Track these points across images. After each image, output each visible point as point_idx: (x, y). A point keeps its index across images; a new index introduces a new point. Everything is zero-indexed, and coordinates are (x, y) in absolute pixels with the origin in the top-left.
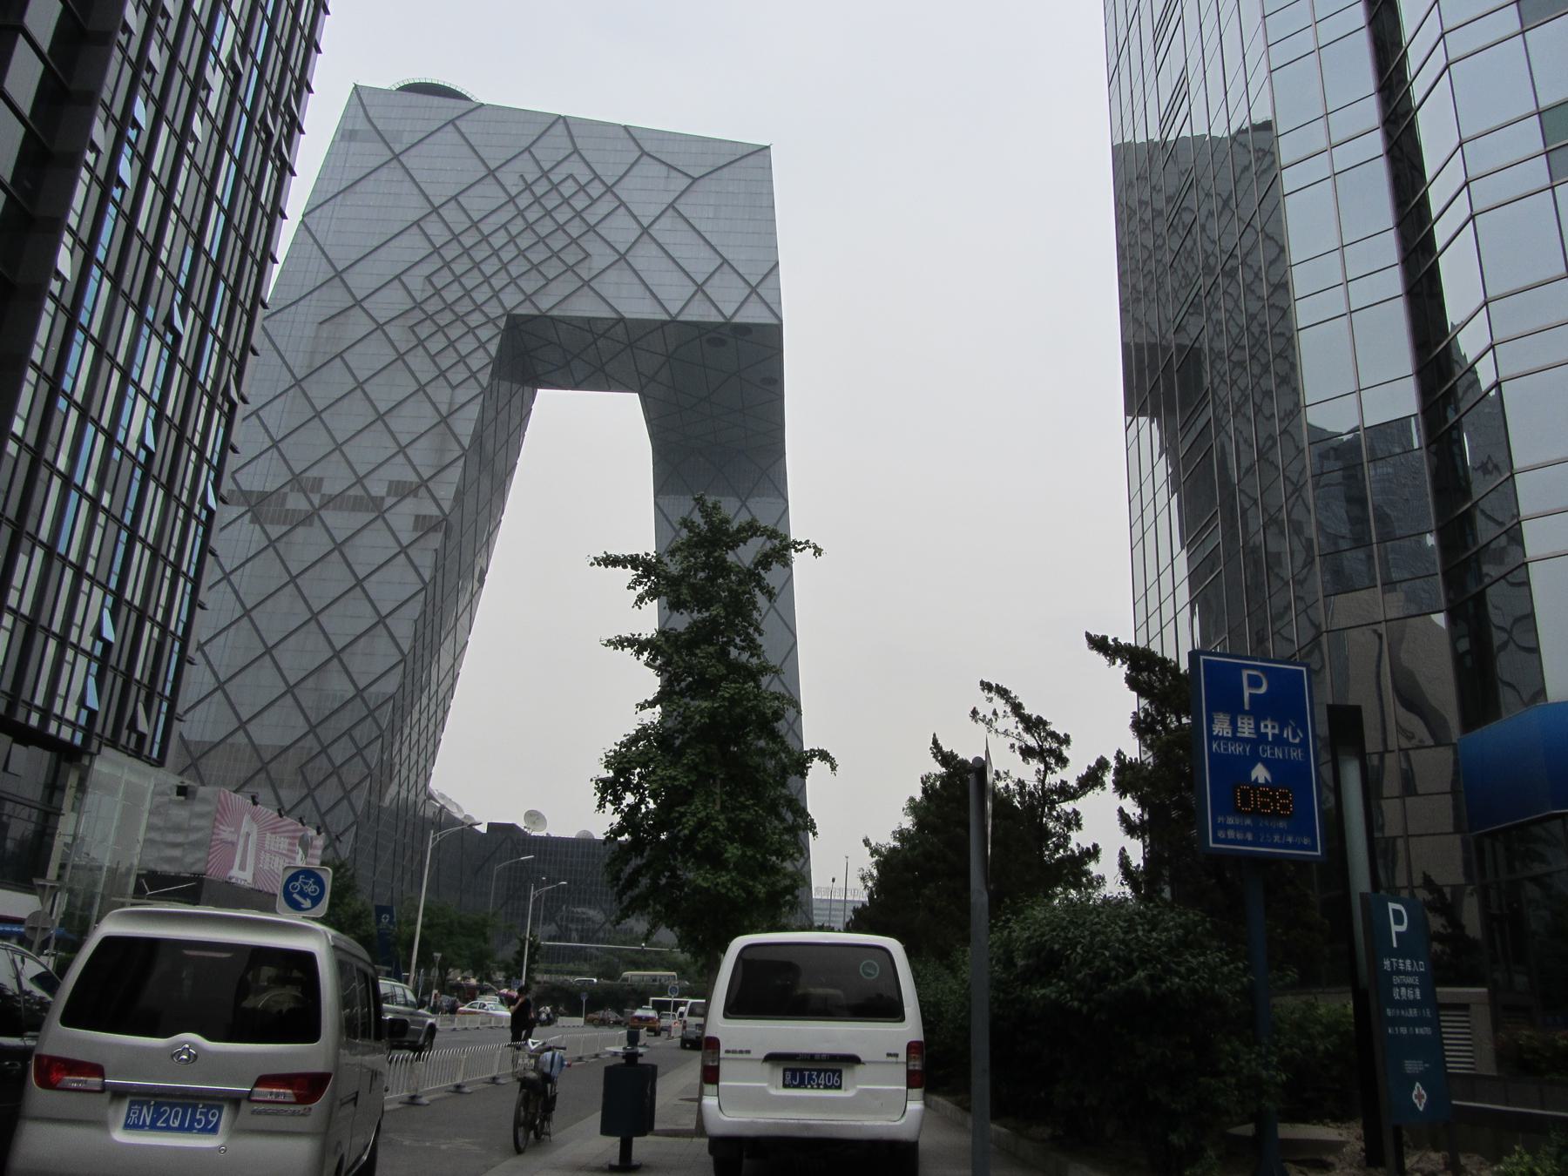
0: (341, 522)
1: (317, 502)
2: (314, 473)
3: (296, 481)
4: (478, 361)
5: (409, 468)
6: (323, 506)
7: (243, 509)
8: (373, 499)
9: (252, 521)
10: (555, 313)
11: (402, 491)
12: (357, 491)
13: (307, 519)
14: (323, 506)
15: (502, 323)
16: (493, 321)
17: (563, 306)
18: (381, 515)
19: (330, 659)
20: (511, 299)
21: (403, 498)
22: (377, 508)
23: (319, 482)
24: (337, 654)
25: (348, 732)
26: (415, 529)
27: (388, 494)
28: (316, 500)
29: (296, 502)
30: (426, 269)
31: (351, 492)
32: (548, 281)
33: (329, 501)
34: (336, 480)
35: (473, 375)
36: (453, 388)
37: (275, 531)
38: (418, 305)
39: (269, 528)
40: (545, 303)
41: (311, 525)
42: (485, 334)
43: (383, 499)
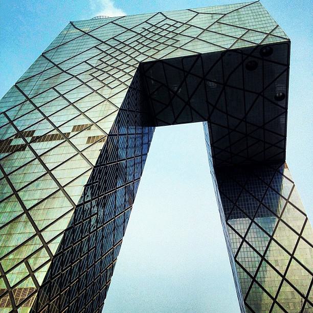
0: (40, 147)
2: (31, 129)
3: (20, 134)
6: (31, 142)
11: (79, 129)
12: (55, 132)
13: (22, 148)
14: (33, 141)
15: (137, 66)
17: (167, 56)
20: (141, 59)
22: (66, 137)
25: (26, 261)
26: (88, 142)
27: (73, 131)
28: (29, 139)
30: (99, 57)
40: (158, 57)
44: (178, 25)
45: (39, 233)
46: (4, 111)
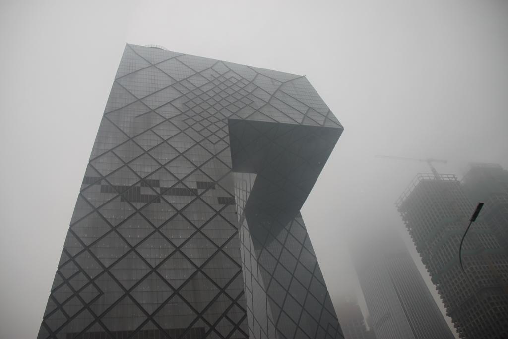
1: (159, 192)
2: (154, 177)
3: (144, 182)
4: (222, 134)
5: (205, 176)
7: (115, 195)
8: (191, 190)
9: (122, 200)
10: (249, 119)
12: (180, 186)
13: (157, 199)
15: (227, 121)
16: (222, 120)
18: (199, 197)
19: (195, 274)
20: (228, 114)
21: (207, 189)
23: (157, 183)
24: (199, 269)
25: (225, 315)
26: (220, 203)
29: (146, 191)
31: (177, 187)
32: (241, 109)
33: (165, 191)
34: (167, 182)
35: (222, 139)
36: (214, 144)
37: (139, 205)
38: (182, 113)
39: (134, 204)
41: (159, 201)
42: (221, 124)
43: (196, 190)
44: (246, 83)
45: (222, 291)
46: (110, 148)
